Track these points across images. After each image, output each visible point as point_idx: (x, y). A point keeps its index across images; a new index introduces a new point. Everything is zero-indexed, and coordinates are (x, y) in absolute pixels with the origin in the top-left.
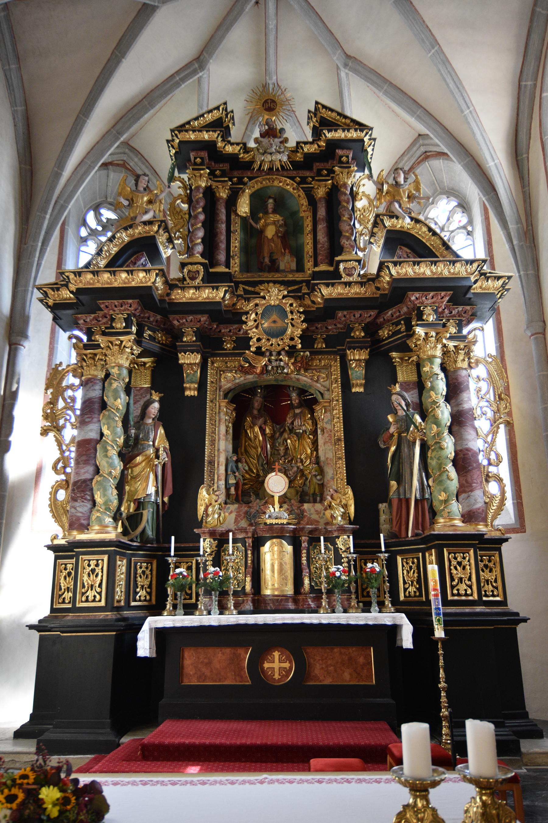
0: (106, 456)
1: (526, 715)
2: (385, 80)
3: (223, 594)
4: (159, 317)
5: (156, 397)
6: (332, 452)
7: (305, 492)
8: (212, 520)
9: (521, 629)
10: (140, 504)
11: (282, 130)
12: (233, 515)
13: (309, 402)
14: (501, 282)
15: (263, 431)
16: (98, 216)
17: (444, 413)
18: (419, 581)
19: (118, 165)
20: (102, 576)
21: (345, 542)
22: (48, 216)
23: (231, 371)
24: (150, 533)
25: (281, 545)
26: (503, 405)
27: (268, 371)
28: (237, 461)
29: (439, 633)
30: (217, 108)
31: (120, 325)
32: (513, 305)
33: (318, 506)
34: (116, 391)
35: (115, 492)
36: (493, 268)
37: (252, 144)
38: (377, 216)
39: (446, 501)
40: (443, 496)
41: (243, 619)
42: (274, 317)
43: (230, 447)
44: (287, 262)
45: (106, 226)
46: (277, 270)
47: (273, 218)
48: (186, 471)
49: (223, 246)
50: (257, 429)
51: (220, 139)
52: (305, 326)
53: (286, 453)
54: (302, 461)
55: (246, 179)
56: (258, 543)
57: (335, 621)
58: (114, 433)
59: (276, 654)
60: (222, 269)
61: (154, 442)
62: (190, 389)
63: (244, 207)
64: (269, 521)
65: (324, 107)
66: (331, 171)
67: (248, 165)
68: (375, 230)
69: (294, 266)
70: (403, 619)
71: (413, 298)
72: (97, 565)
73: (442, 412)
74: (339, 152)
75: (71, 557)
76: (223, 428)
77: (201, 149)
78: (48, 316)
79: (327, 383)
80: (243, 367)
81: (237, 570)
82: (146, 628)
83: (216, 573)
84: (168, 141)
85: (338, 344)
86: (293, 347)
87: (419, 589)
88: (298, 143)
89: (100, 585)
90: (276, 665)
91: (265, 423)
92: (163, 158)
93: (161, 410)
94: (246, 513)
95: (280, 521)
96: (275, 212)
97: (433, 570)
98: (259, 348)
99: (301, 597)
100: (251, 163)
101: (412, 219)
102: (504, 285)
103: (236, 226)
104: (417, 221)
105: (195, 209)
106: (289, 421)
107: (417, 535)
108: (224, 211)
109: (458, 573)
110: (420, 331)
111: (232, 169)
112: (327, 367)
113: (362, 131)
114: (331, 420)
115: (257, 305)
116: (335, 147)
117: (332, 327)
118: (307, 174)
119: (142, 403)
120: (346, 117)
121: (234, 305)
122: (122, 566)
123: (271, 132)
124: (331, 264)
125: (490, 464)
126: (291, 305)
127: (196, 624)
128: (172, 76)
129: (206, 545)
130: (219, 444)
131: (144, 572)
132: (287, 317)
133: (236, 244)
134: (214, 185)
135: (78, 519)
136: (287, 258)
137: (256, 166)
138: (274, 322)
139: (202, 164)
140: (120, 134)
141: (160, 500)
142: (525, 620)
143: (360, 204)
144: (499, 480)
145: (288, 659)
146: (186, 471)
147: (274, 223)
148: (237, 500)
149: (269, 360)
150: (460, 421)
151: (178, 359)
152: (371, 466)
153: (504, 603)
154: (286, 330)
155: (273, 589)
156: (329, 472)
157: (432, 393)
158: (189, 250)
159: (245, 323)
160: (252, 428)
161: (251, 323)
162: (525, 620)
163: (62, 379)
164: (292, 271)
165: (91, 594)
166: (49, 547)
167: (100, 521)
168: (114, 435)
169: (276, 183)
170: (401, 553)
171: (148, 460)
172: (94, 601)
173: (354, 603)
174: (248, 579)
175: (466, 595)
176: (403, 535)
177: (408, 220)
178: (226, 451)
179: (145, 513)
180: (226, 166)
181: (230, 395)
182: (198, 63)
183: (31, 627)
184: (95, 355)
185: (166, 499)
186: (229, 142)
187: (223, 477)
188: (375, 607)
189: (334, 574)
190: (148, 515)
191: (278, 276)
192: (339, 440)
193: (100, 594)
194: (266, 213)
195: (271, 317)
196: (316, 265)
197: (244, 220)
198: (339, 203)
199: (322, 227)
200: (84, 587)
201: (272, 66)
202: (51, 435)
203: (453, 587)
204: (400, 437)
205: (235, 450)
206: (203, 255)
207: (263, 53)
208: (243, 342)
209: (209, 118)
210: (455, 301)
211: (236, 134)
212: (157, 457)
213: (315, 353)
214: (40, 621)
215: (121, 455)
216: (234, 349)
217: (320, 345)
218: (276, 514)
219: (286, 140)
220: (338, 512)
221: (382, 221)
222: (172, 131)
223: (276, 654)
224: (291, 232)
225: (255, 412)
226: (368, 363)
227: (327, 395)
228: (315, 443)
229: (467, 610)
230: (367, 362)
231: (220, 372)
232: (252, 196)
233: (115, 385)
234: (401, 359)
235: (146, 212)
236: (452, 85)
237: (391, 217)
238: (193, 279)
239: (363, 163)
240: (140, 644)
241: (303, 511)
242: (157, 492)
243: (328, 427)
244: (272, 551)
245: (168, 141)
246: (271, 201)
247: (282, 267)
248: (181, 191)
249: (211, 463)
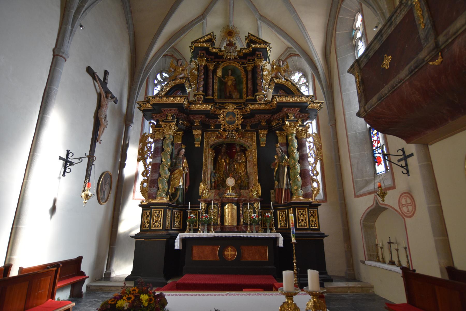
0: (163, 170)
1: (326, 273)
2: (275, 25)
3: (209, 225)
4: (185, 115)
5: (183, 147)
6: (253, 170)
8: (205, 195)
9: (325, 239)
10: (176, 189)
11: (235, 44)
12: (213, 194)
14: (319, 105)
16: (161, 76)
17: (297, 155)
18: (286, 221)
19: (170, 56)
20: (161, 217)
21: (257, 205)
22: (142, 75)
23: (213, 137)
24: (180, 200)
25: (232, 206)
26: (319, 153)
27: (228, 138)
28: (215, 173)
29: (294, 241)
30: (210, 34)
31: (170, 118)
32: (323, 114)
33: (247, 191)
34: (168, 144)
35: (167, 184)
36: (316, 99)
37: (223, 49)
38: (272, 78)
39: (297, 190)
40: (296, 188)
41: (217, 235)
42: (231, 116)
43: (212, 167)
44: (236, 95)
45: (165, 79)
46: (232, 98)
47: (231, 78)
48: (194, 177)
49: (211, 88)
50: (223, 160)
51: (210, 46)
52: (243, 120)
53: (234, 170)
54: (240, 173)
55: (220, 62)
56: (223, 205)
57: (253, 236)
58: (166, 160)
59: (230, 249)
60: (210, 97)
61: (182, 165)
62: (197, 144)
63: (219, 73)
64: (227, 197)
65: (251, 35)
66: (254, 60)
67: (221, 57)
68: (271, 83)
69: (239, 97)
70: (280, 236)
71: (285, 110)
72: (159, 213)
73: (296, 155)
74: (257, 53)
75: (149, 210)
76: (210, 160)
77: (203, 50)
78: (141, 114)
79: (251, 143)
80: (218, 136)
81: (215, 216)
82: (178, 237)
83: (206, 216)
84: (190, 47)
85: (256, 128)
86: (238, 128)
87: (286, 224)
88: (241, 49)
89: (160, 221)
90: (230, 253)
91: (226, 158)
92: (188, 54)
93: (185, 152)
94: (218, 193)
95: (232, 197)
96: (231, 75)
97: (292, 216)
98: (224, 129)
99: (239, 226)
101: (285, 79)
102: (320, 105)
103: (216, 81)
104: (287, 80)
105: (200, 73)
106: (236, 157)
107: (285, 203)
108: (211, 74)
109: (301, 217)
111: (215, 58)
112: (251, 137)
113: (266, 45)
114: (253, 157)
115: (224, 111)
116: (255, 50)
117: (253, 121)
118: (244, 61)
119: (178, 149)
120: (260, 39)
121: (215, 111)
122: (169, 213)
123: (231, 44)
124: (253, 95)
125: (314, 175)
126: (237, 112)
127: (198, 236)
128: (192, 21)
129: (202, 205)
130: (208, 166)
131: (177, 216)
132: (236, 116)
133: (216, 88)
134: (208, 64)
135: (152, 194)
136: (236, 93)
137: (224, 57)
138: (231, 118)
139: (203, 56)
140: (171, 43)
141: (184, 188)
142: (327, 236)
143: (265, 73)
144: (317, 182)
145: (234, 250)
146: (194, 177)
147: (231, 80)
148: (215, 188)
149: (228, 133)
150: (303, 158)
151: (192, 132)
152: (268, 176)
153: (318, 229)
154: (235, 121)
155: (229, 223)
156: (251, 178)
157: (292, 147)
158: (198, 90)
159: (219, 118)
160: (221, 160)
161: (221, 119)
162: (327, 236)
163: (146, 139)
164: (238, 99)
165: (156, 224)
166: (140, 206)
167: (161, 195)
168: (166, 161)
169: (232, 64)
170: (279, 209)
171: (180, 172)
172: (158, 227)
173: (260, 229)
174: (219, 219)
175: (304, 226)
176: (280, 202)
177: (284, 80)
178: (211, 169)
179: (178, 192)
180: (213, 57)
181: (213, 147)
182: (202, 17)
183: (132, 237)
184: (160, 130)
185: (187, 187)
186: (214, 48)
187: (209, 179)
188: (269, 231)
189: (253, 217)
190: (179, 193)
191: (232, 101)
192: (255, 165)
193: (160, 224)
194: (228, 76)
195: (229, 117)
196: (247, 96)
197: (219, 78)
198: (257, 72)
199: (250, 82)
200: (154, 221)
201: (231, 19)
202: (141, 161)
203: (299, 223)
204: (279, 164)
205: (214, 169)
206: (203, 91)
207: (228, 14)
209: (206, 38)
210: (301, 112)
211: (217, 44)
212: (184, 170)
213: (246, 131)
214: (136, 235)
215: (169, 169)
216: (215, 128)
217: (248, 128)
218: (230, 193)
219: (236, 47)
220: (255, 193)
221: (273, 80)
222: (192, 42)
223: (230, 249)
224: (238, 83)
225: (223, 154)
227: (251, 147)
229: (304, 232)
230: (267, 135)
231: (209, 137)
232: (222, 69)
233: (167, 142)
234: (280, 134)
235: (181, 74)
236: (301, 28)
237: (277, 78)
238: (199, 101)
239: (266, 57)
240: (176, 244)
241: (241, 193)
242: (183, 184)
243: (251, 160)
244: (228, 208)
245: (190, 47)
246: (230, 71)
247: (234, 97)
248: (195, 66)
249: (205, 173)
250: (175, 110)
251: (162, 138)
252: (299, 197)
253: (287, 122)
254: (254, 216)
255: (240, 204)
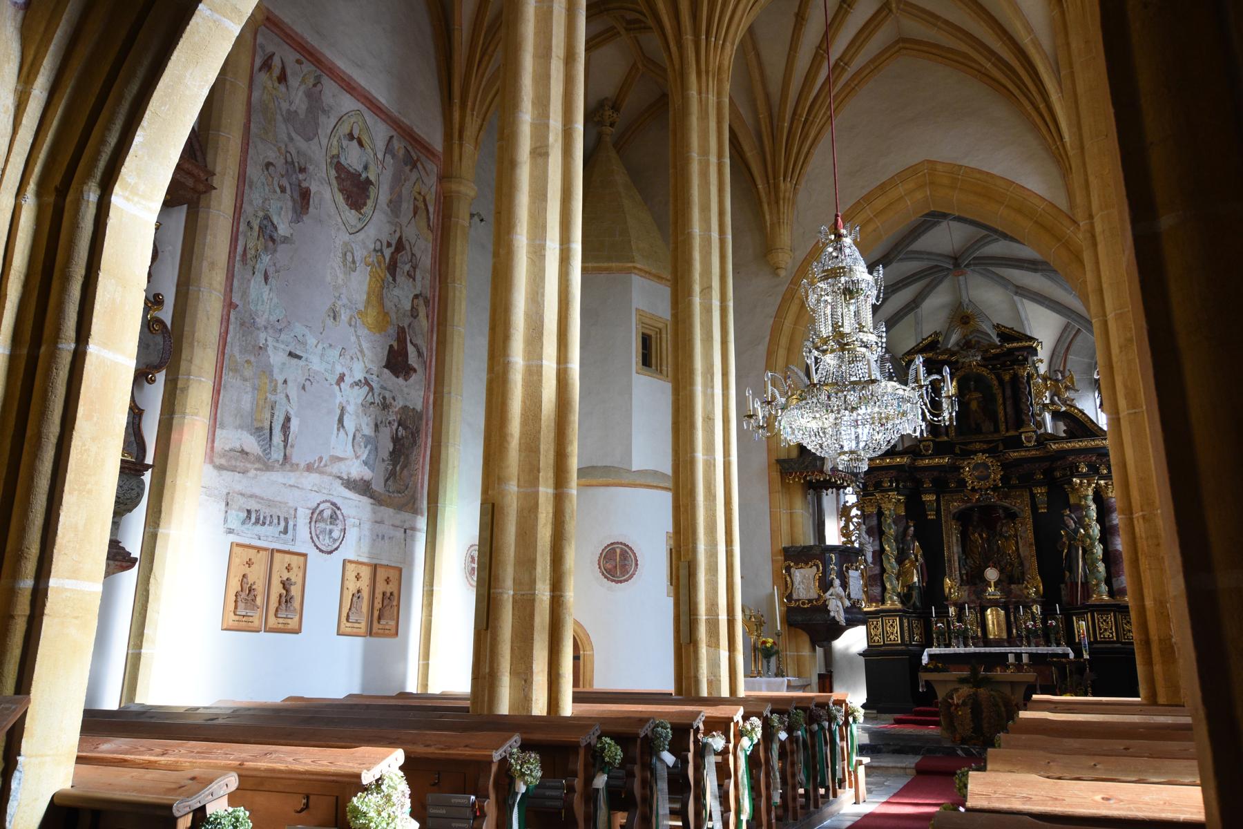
2: (1046, 298)
6: (1028, 552)
7: (1008, 579)
10: (910, 587)
13: (1012, 516)
15: (981, 536)
21: (1037, 609)
29: (1086, 656)
39: (1098, 585)
41: (978, 650)
44: (987, 426)
47: (977, 395)
48: (934, 569)
69: (992, 429)
70: (1070, 650)
85: (1027, 482)
100: (957, 362)
104: (1071, 406)
109: (1104, 626)
110: (1076, 480)
114: (1026, 530)
129: (952, 610)
130: (953, 549)
137: (960, 365)
146: (934, 569)
152: (1055, 559)
156: (1027, 565)
167: (891, 599)
171: (913, 564)
190: (915, 593)
191: (981, 437)
195: (980, 472)
199: (1009, 403)
204: (1070, 544)
205: (964, 551)
208: (962, 483)
217: (1014, 482)
226: (1049, 494)
228: (1017, 543)
249: (949, 561)
250: (894, 473)
251: (875, 511)
252: (1102, 594)
253: (1076, 480)
254: (1030, 624)
255: (1009, 606)
